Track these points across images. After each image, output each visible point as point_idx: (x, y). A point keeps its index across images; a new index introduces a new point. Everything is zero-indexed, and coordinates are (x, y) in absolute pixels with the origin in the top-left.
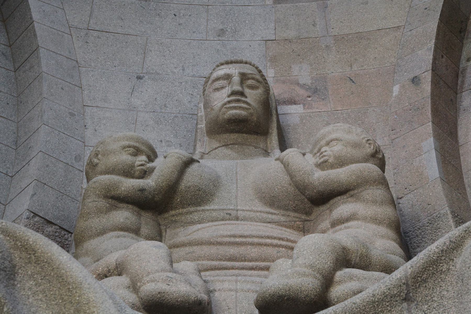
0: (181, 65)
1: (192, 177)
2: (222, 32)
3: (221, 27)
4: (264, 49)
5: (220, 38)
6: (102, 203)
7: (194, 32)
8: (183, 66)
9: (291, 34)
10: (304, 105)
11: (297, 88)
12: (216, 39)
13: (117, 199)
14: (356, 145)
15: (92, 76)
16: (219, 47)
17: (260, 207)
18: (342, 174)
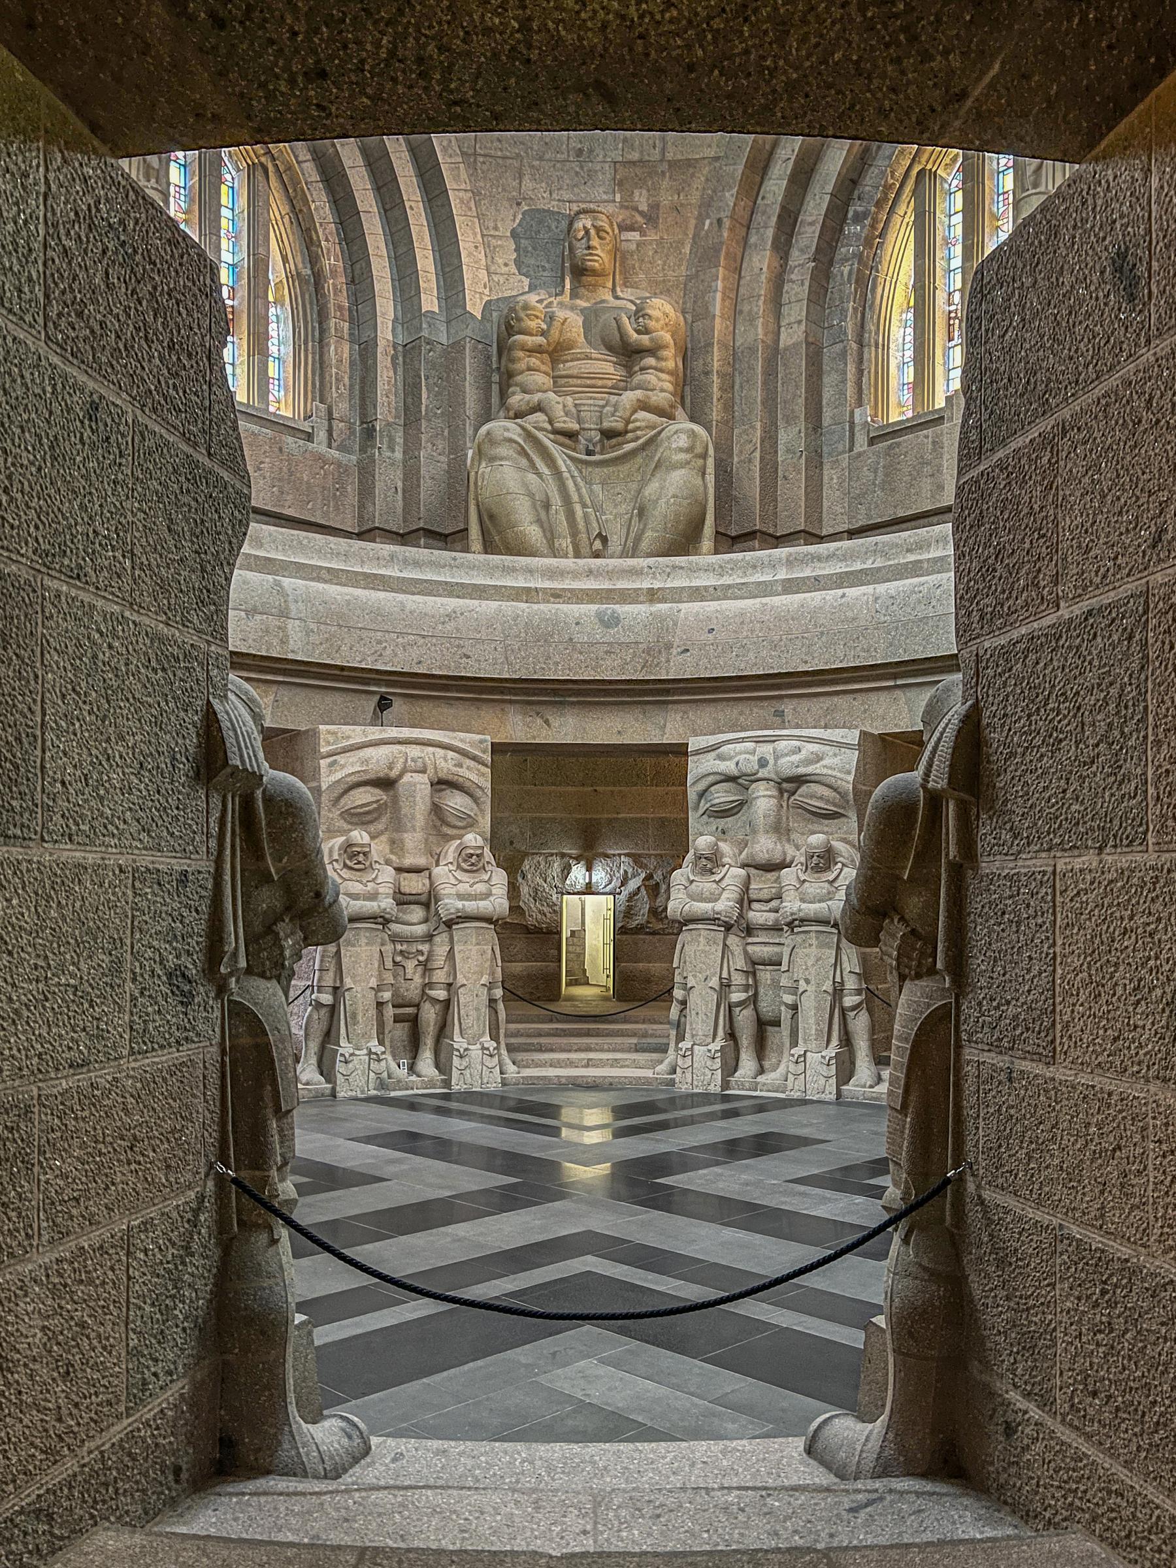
9: (635, 156)
11: (637, 215)
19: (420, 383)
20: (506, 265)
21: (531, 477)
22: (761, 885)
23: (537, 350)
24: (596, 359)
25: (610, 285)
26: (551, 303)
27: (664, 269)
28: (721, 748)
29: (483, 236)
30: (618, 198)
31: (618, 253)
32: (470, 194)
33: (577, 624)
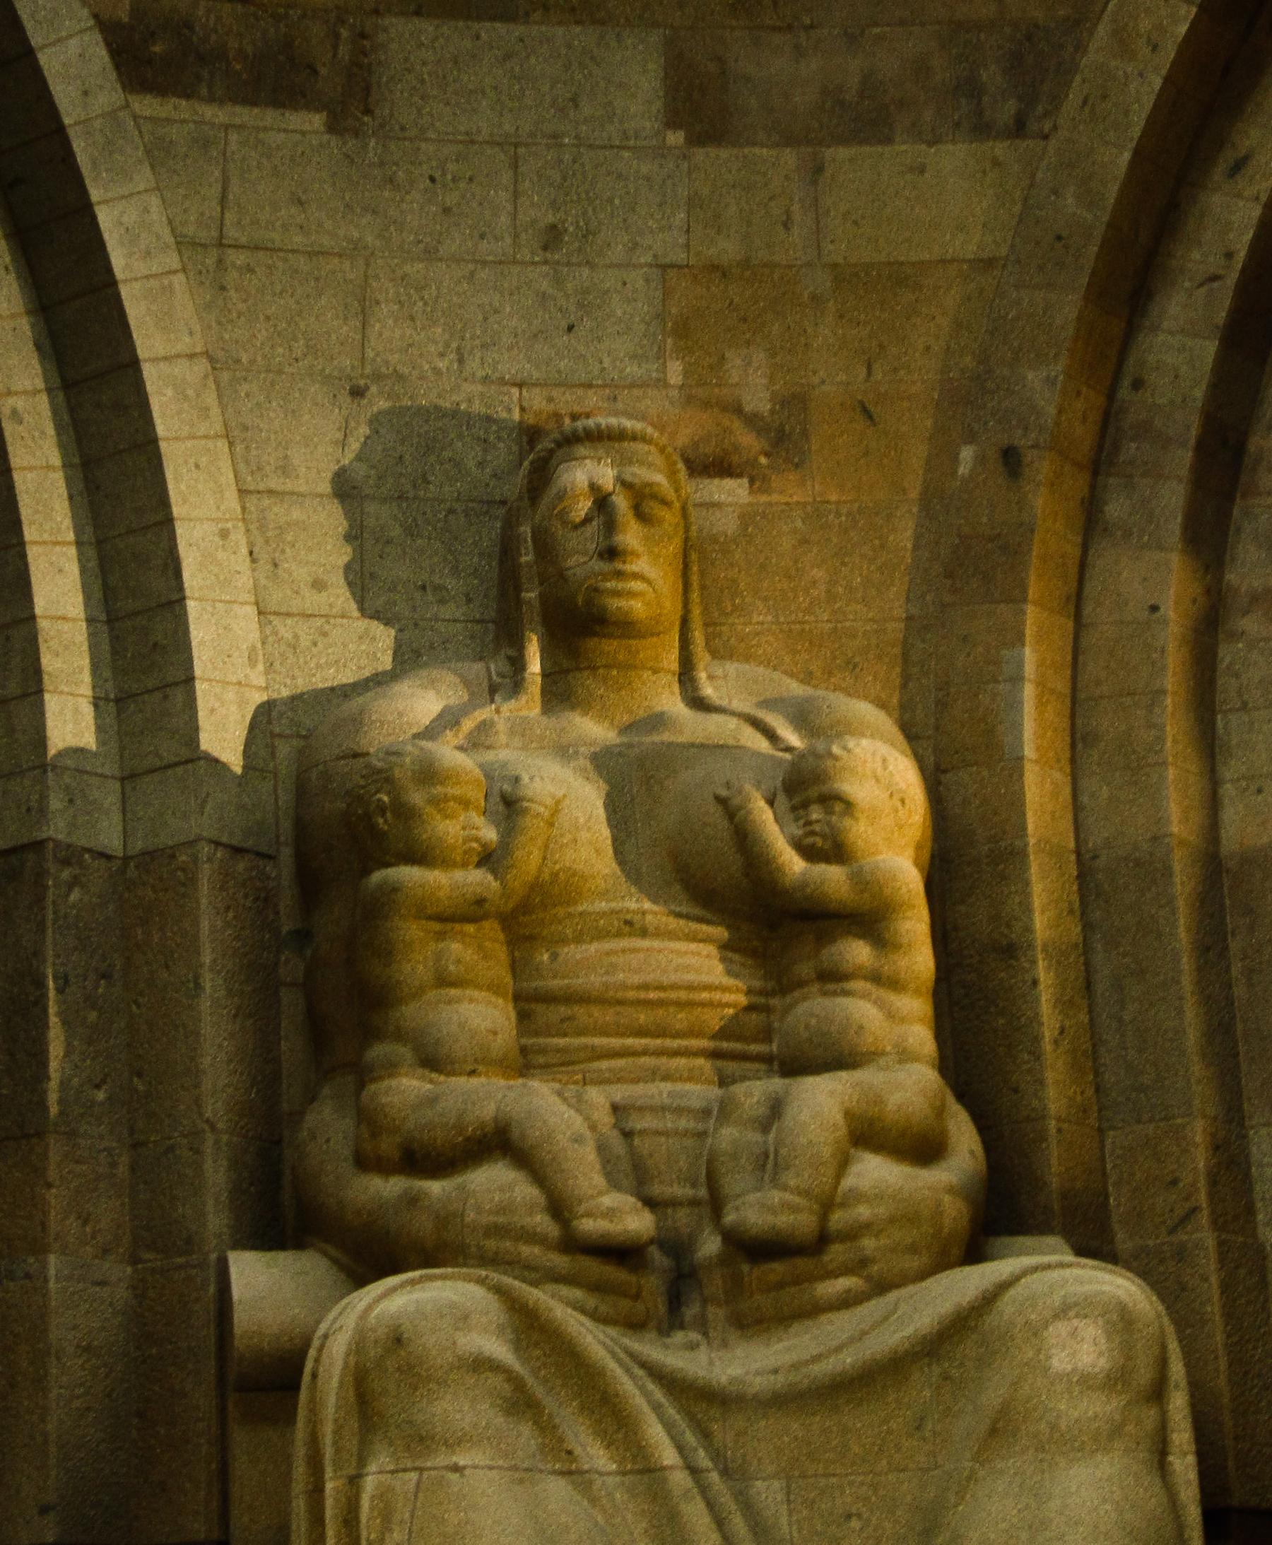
0: (454, 345)
2: (552, 237)
3: (551, 219)
4: (659, 294)
5: (549, 255)
7: (482, 236)
8: (458, 349)
9: (727, 249)
10: (752, 481)
11: (737, 425)
12: (537, 259)
15: (247, 395)
16: (545, 285)
19: (41, 1003)
20: (318, 585)
21: (557, 1490)
23: (472, 911)
24: (659, 934)
25: (671, 660)
26: (484, 727)
27: (831, 597)
29: (243, 492)
30: (675, 371)
31: (694, 558)
32: (202, 366)
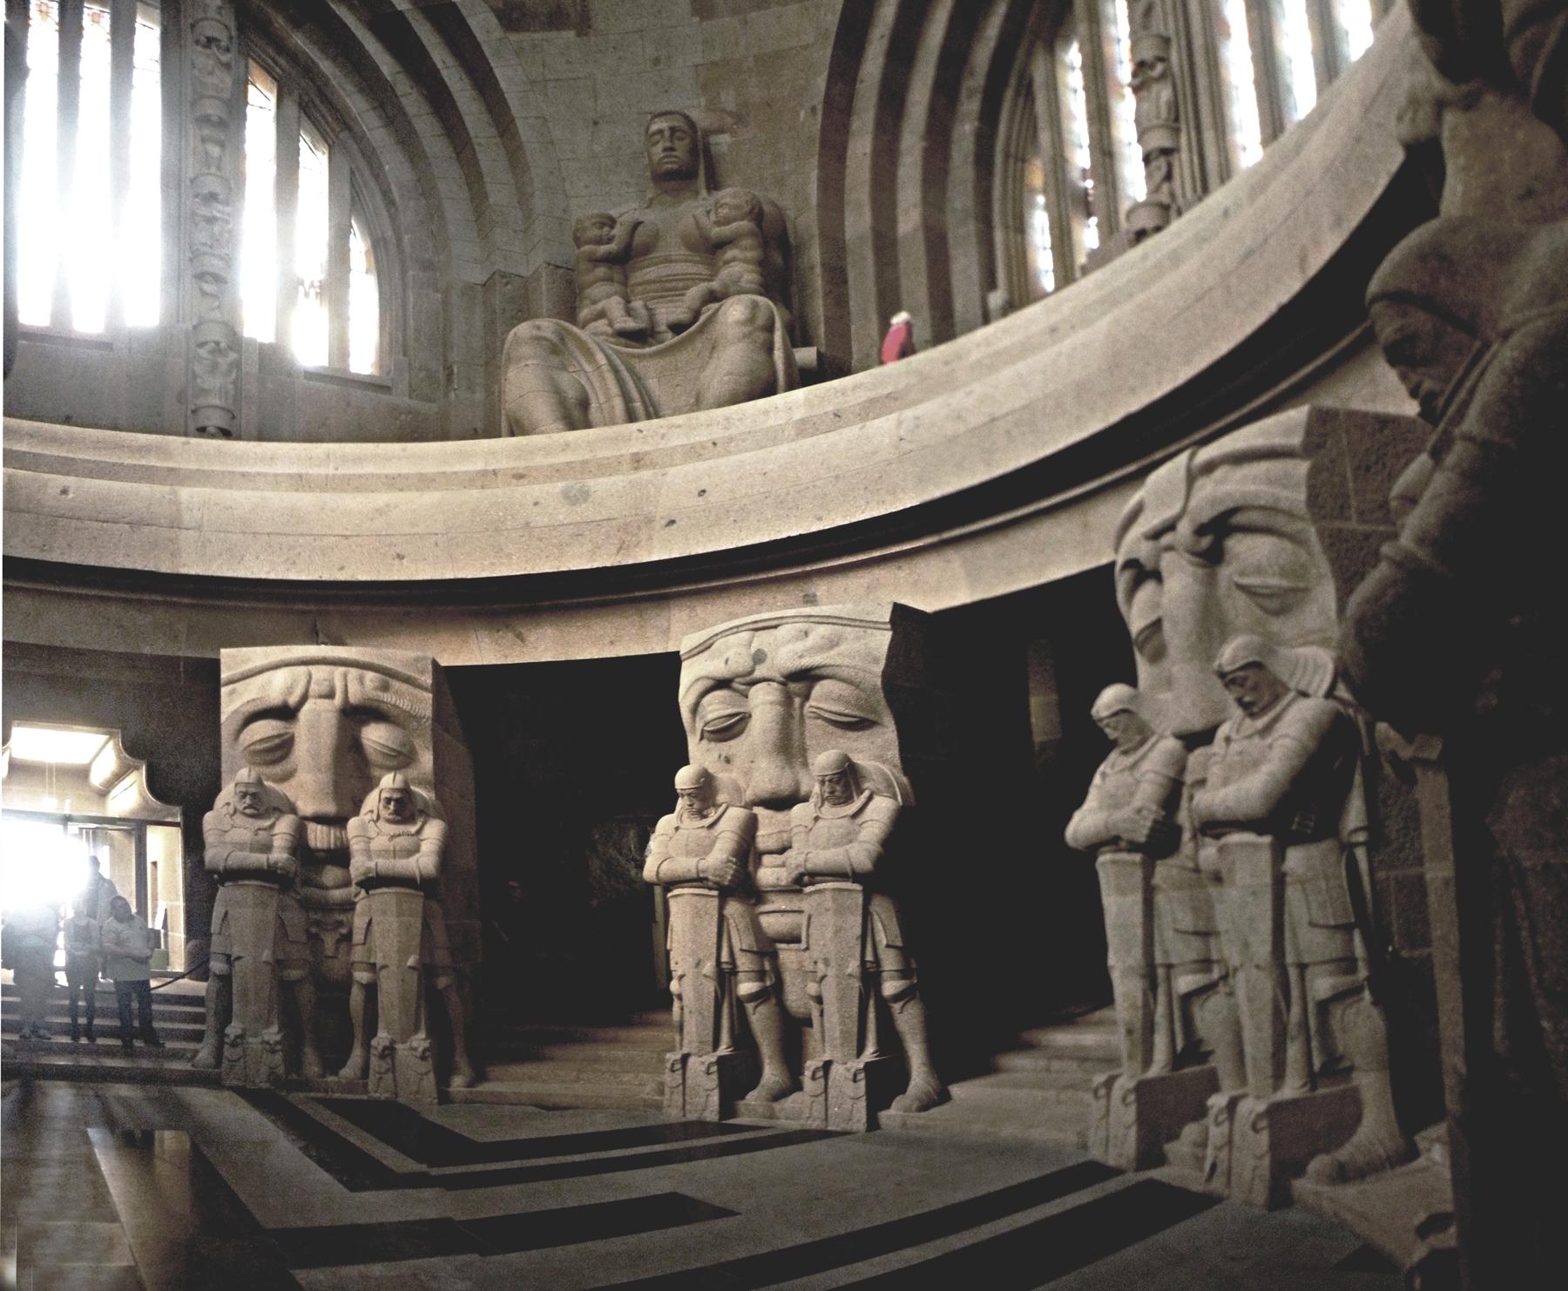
1: (639, 238)
6: (590, 265)
13: (597, 261)
14: (738, 207)
17: (683, 251)
18: (726, 230)
22: (770, 826)
28: (707, 643)
30: (703, 101)
33: (536, 504)
